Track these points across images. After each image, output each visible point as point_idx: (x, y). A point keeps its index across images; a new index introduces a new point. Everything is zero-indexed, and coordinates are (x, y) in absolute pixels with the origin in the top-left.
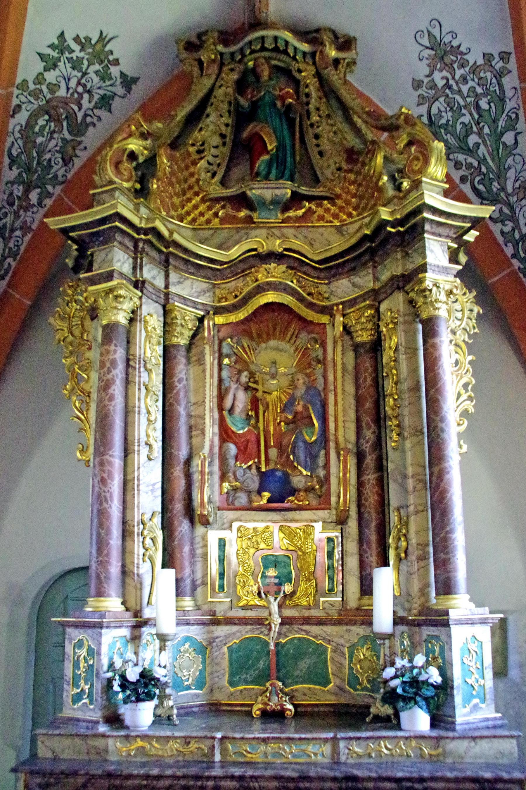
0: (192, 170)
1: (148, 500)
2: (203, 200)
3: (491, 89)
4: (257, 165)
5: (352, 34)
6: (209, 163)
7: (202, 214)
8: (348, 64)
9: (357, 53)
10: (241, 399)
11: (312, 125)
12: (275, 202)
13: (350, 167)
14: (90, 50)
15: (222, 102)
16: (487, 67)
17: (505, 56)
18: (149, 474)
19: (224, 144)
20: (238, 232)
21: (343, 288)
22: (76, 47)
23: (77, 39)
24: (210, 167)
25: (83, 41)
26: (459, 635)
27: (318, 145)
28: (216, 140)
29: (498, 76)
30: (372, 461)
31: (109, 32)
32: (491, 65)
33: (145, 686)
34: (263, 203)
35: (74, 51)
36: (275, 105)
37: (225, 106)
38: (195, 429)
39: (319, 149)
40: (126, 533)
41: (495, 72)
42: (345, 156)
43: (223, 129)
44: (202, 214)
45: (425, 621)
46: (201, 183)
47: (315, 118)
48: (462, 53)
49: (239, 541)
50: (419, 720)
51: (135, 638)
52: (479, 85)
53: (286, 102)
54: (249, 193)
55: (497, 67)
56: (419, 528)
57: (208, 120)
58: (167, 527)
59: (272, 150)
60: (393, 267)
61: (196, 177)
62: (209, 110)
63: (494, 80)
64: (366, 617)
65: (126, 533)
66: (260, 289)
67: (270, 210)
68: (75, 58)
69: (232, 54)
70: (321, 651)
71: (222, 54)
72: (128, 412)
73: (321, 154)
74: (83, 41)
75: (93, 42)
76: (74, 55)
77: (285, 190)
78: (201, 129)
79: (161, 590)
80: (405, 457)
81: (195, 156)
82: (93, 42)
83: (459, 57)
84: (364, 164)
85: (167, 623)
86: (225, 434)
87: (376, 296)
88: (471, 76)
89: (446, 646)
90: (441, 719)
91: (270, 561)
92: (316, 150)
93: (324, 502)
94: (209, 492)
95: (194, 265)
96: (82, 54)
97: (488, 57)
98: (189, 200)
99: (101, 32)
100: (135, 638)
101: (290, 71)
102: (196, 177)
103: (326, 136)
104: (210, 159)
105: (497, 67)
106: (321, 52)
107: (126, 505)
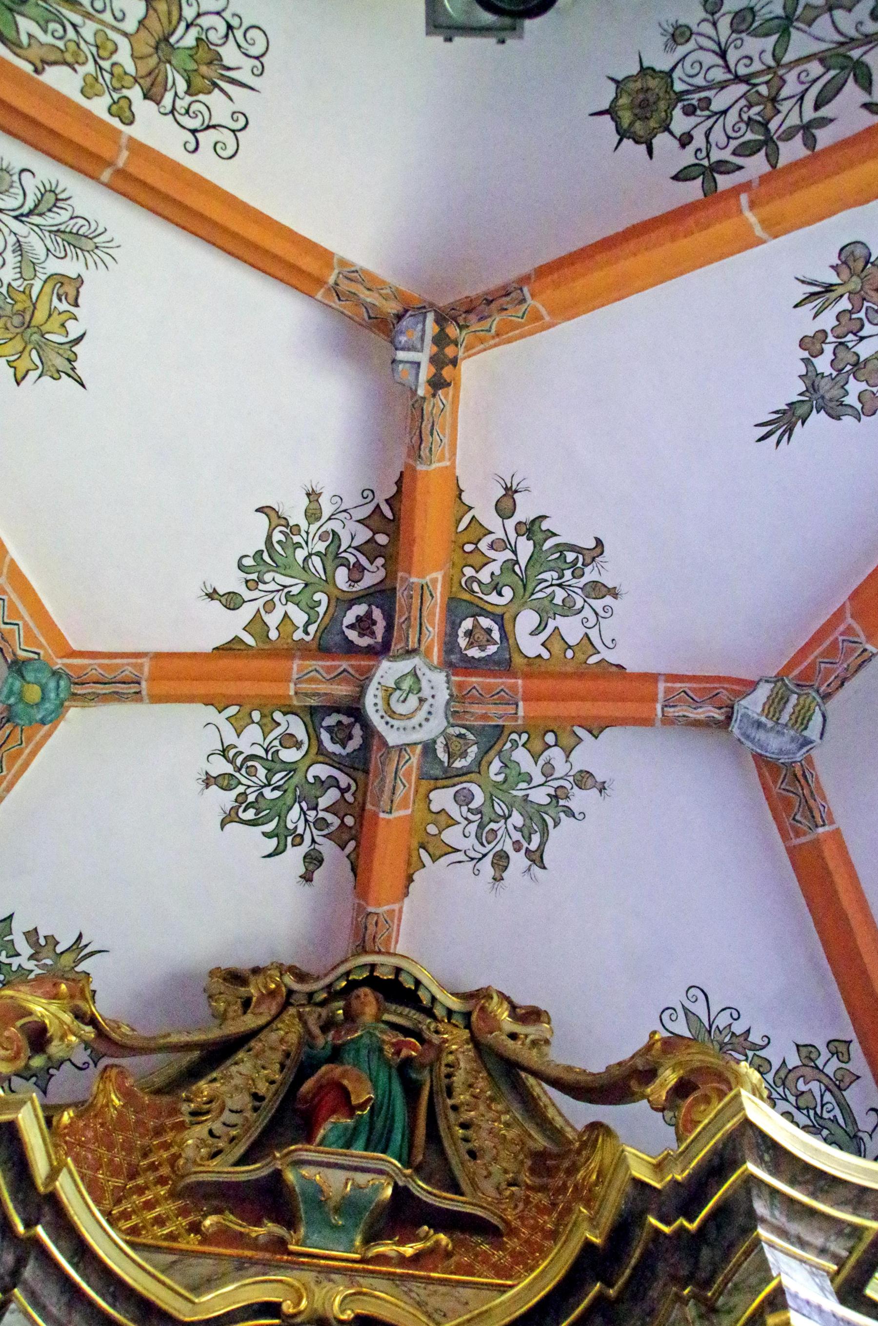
0: (168, 1137)
2: (173, 1195)
3: (826, 1115)
4: (322, 1132)
5: (543, 1007)
6: (211, 1133)
7: (160, 1221)
8: (534, 1043)
9: (552, 1030)
11: (455, 1108)
12: (349, 1206)
13: (538, 1181)
14: (49, 962)
15: (271, 1048)
16: (807, 1071)
17: (842, 1048)
19: (255, 1109)
20: (240, 1268)
22: (25, 950)
23: (32, 935)
24: (210, 1141)
25: (42, 942)
27: (466, 1140)
28: (241, 1100)
29: (835, 1089)
31: (94, 939)
32: (817, 1067)
34: (317, 1199)
35: (18, 955)
36: (381, 1050)
37: (278, 1056)
39: (470, 1145)
41: (826, 1080)
42: (529, 1162)
43: (262, 1088)
44: (160, 1221)
46: (181, 1162)
47: (462, 1097)
48: (756, 1047)
52: (798, 1108)
53: (404, 1053)
54: (290, 1176)
55: (829, 1070)
57: (234, 1069)
59: (362, 1106)
61: (173, 1150)
62: (241, 1055)
63: (828, 1097)
67: (334, 1227)
68: (14, 968)
69: (310, 995)
71: (290, 992)
73: (472, 1154)
74: (42, 942)
75: (59, 949)
76: (15, 962)
77: (380, 1177)
78: (214, 1080)
81: (187, 1119)
82: (59, 949)
83: (750, 1054)
84: (572, 1171)
88: (780, 1090)
92: (463, 1147)
96: (30, 965)
97: (806, 1050)
98: (141, 1190)
99: (80, 936)
101: (421, 1030)
102: (173, 1150)
103: (484, 1125)
104: (217, 1127)
105: (829, 1070)
106: (483, 1009)
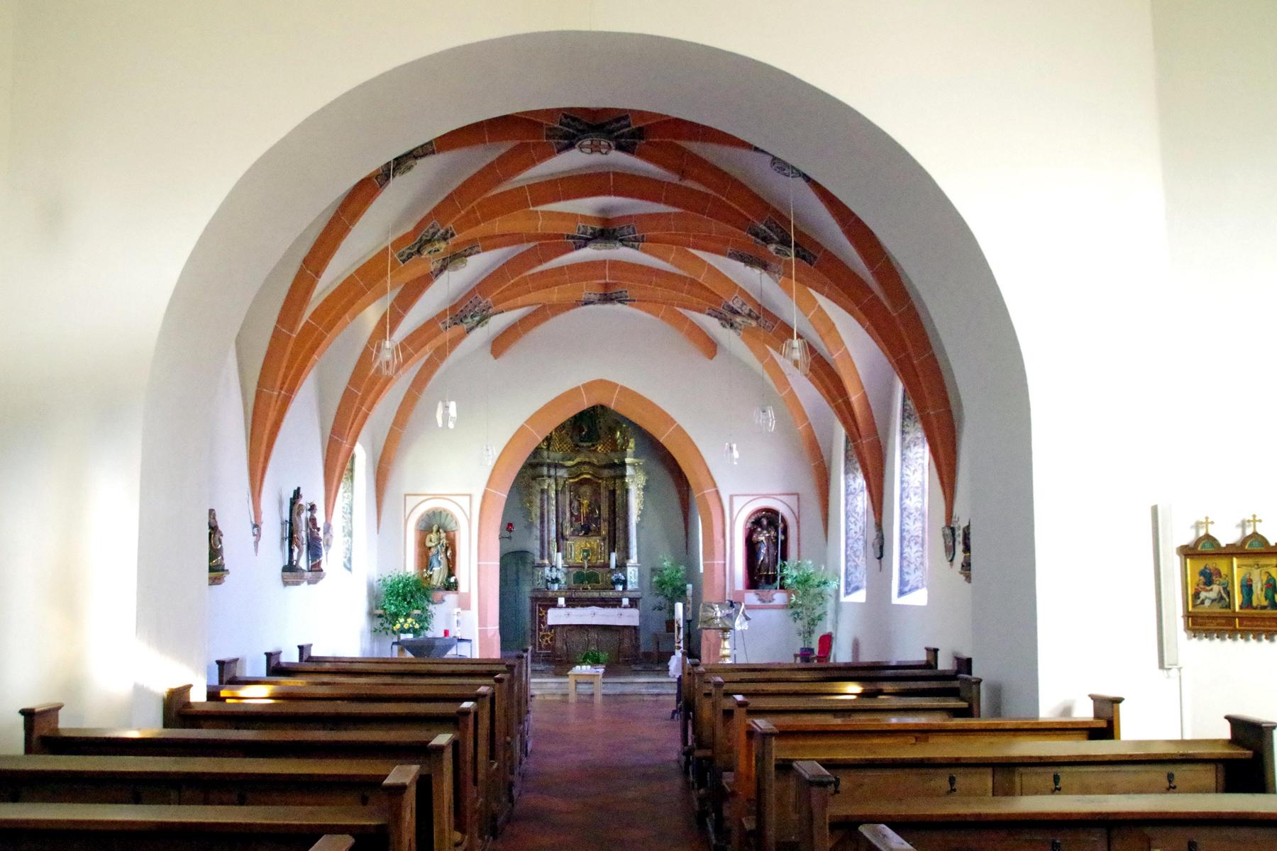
1: (553, 535)
10: (576, 504)
18: (553, 528)
21: (606, 473)
33: (556, 580)
45: (622, 566)
49: (577, 546)
50: (620, 588)
79: (558, 559)
80: (620, 525)
87: (614, 478)
90: (625, 589)
94: (567, 532)
95: (563, 466)
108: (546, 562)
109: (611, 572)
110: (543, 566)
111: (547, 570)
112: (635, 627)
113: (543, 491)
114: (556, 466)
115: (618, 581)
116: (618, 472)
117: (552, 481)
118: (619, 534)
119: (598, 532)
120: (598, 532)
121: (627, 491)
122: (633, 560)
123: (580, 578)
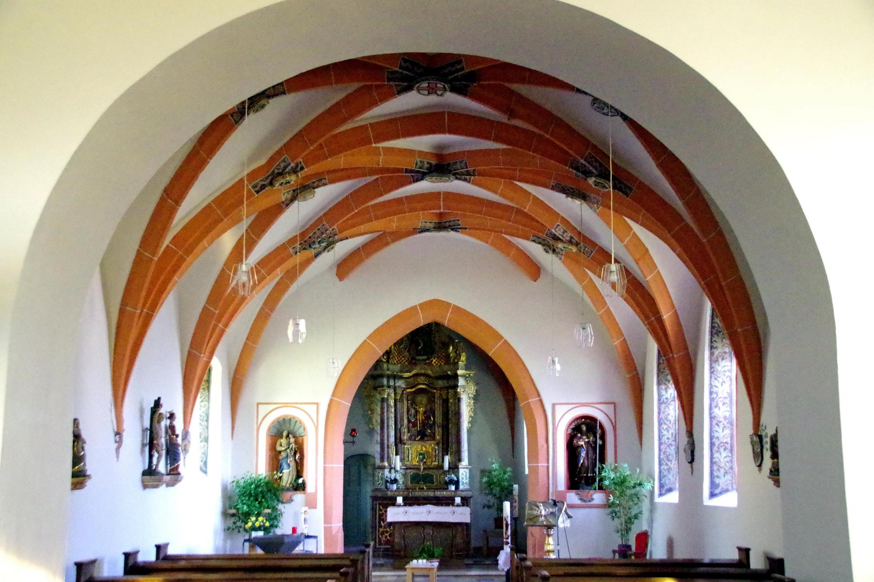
1: (392, 439)
10: (413, 411)
18: (392, 433)
26: (461, 471)
30: (445, 428)
33: (395, 481)
38: (402, 419)
40: (388, 447)
45: (454, 468)
49: (414, 449)
50: (453, 488)
51: (390, 472)
56: (454, 447)
58: (396, 445)
60: (451, 383)
64: (442, 467)
65: (388, 447)
66: (419, 384)
70: (432, 476)
72: (388, 418)
85: (398, 468)
86: (409, 421)
87: (448, 388)
89: (458, 472)
90: (457, 488)
91: (420, 454)
93: (434, 438)
94: (405, 437)
95: (401, 378)
100: (390, 472)
107: (388, 441)
108: (386, 464)
109: (445, 473)
110: (383, 468)
111: (386, 471)
112: (466, 524)
113: (383, 400)
114: (395, 377)
115: (451, 482)
116: (451, 383)
117: (391, 391)
118: (452, 439)
119: (433, 438)
120: (433, 438)
121: (459, 400)
122: (465, 462)
123: (416, 479)
